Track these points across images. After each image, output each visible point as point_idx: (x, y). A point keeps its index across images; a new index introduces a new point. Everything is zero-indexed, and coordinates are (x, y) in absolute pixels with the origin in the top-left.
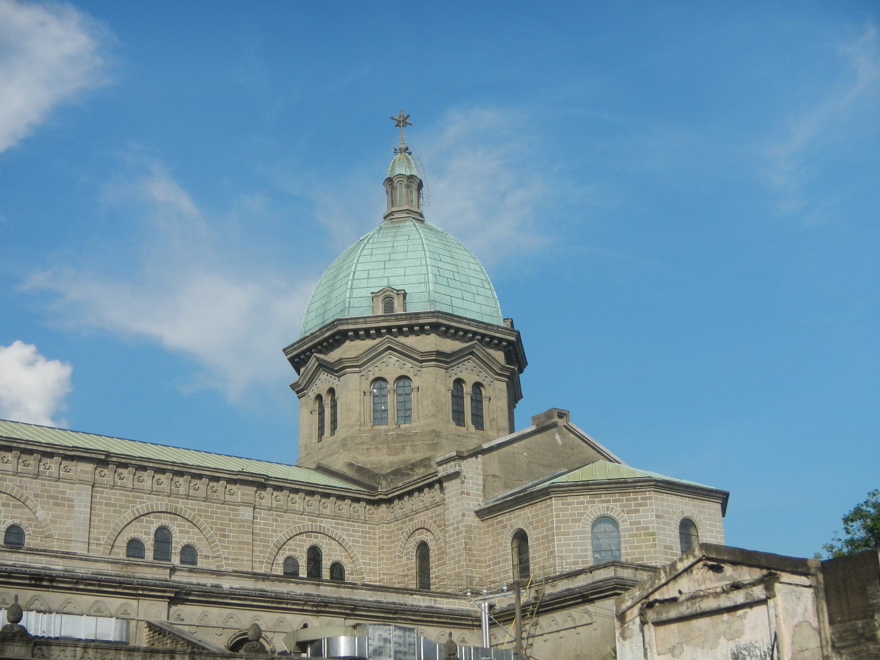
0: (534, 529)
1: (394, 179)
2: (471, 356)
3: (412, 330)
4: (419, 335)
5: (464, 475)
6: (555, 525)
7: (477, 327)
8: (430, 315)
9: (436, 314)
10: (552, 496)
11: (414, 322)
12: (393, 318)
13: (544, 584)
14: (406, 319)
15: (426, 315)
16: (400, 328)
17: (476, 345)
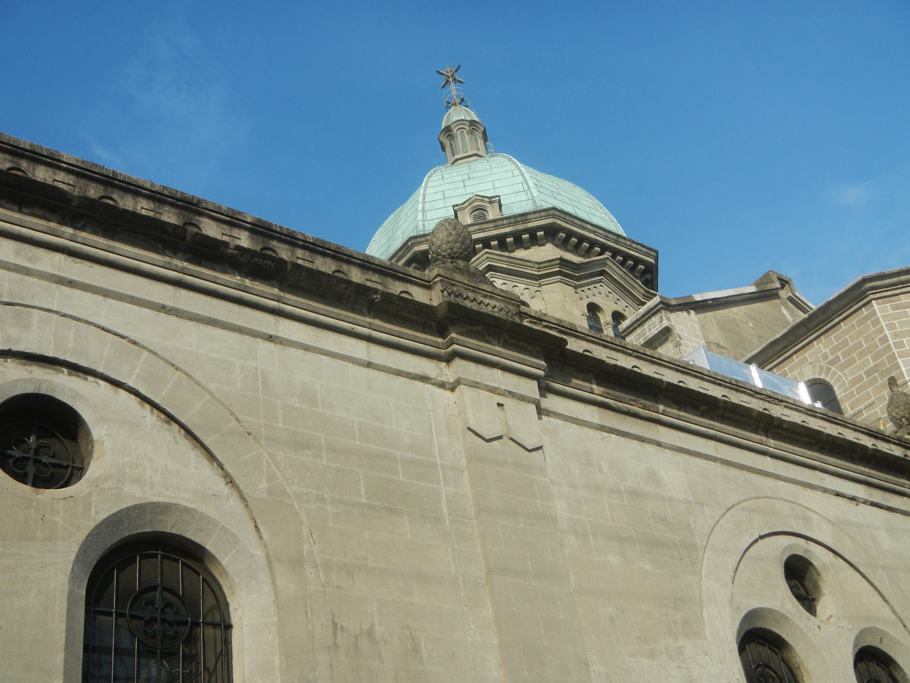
0: (842, 368)
1: (452, 127)
2: (602, 277)
3: (519, 243)
4: (529, 248)
5: (678, 334)
6: (891, 342)
8: (543, 214)
9: (552, 212)
10: (872, 297)
11: (521, 227)
12: (491, 226)
14: (509, 225)
15: (538, 215)
16: (501, 239)
17: (608, 262)
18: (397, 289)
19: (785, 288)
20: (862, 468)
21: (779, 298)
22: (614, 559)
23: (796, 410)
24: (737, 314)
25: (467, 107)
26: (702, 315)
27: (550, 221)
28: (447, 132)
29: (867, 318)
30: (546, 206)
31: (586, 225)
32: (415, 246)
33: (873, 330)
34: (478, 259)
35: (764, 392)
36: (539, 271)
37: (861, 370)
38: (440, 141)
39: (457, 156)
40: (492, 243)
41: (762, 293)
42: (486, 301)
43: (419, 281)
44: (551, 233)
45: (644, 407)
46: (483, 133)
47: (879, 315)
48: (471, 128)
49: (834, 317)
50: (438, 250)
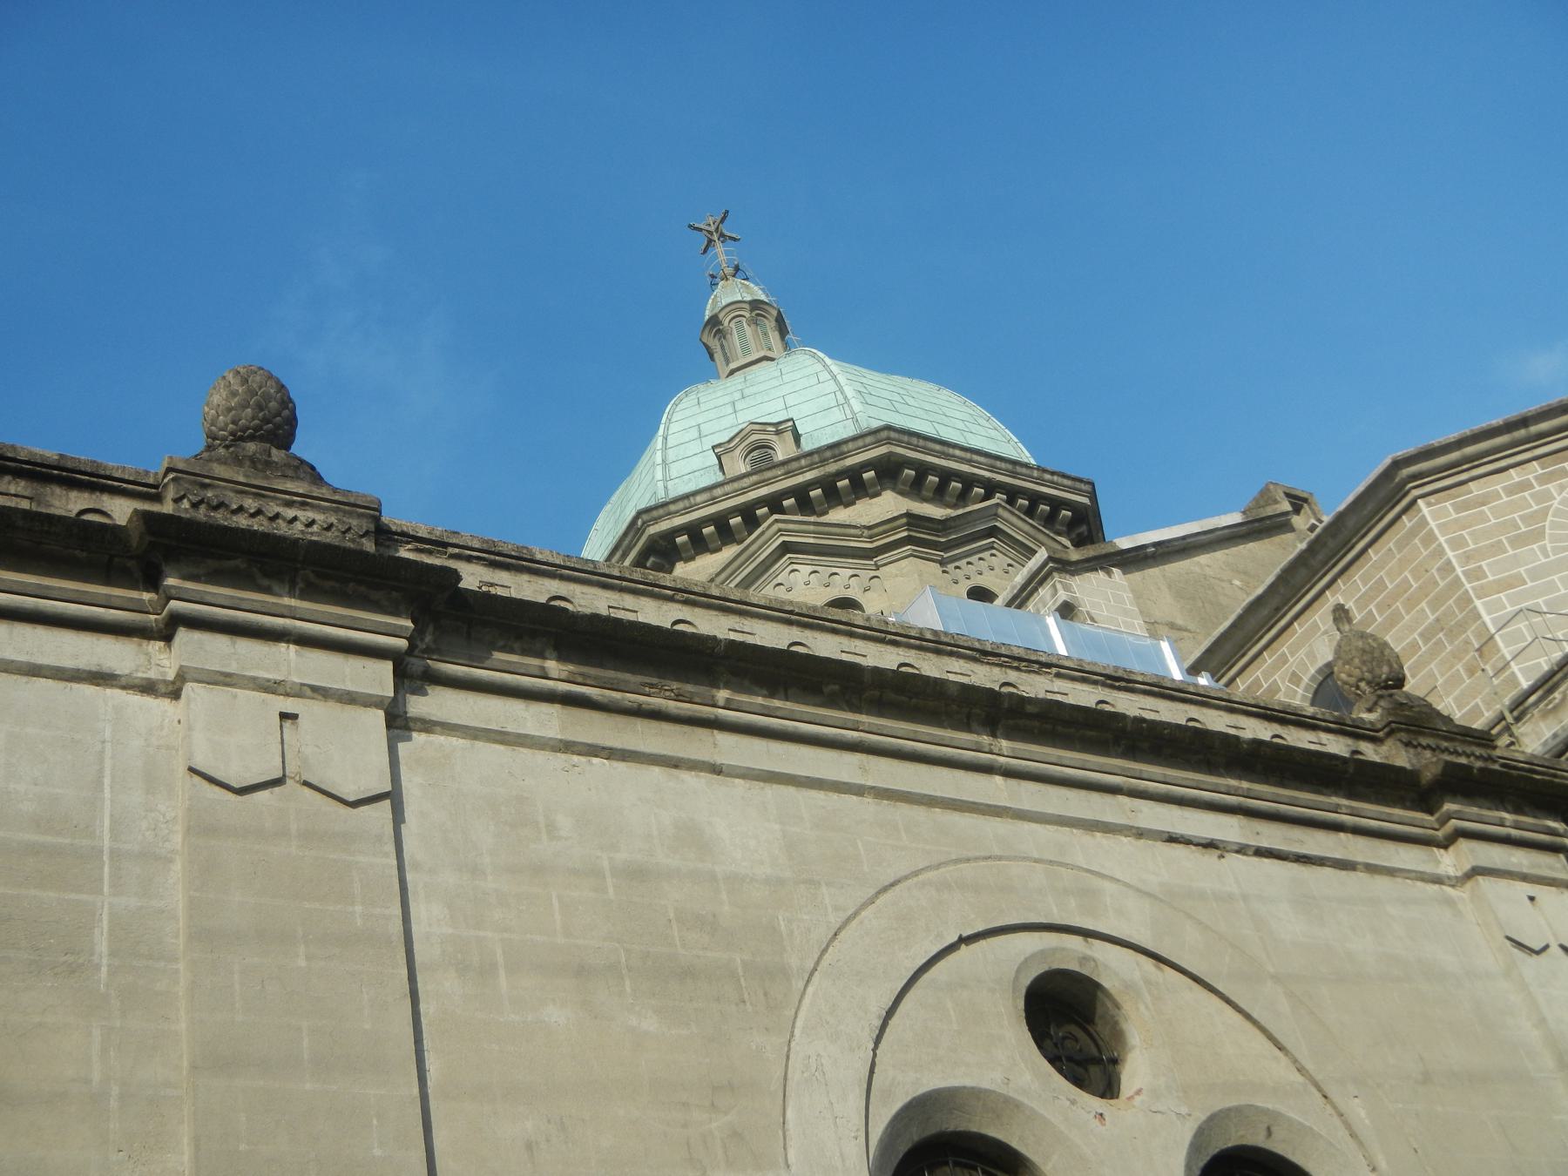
1: (721, 316)
2: (993, 539)
3: (834, 497)
4: (852, 503)
5: (1088, 613)
6: (1459, 571)
7: (992, 469)
8: (869, 440)
9: (884, 434)
10: (1416, 493)
11: (832, 468)
13: (1507, 714)
14: (811, 467)
15: (860, 443)
16: (800, 493)
17: (1000, 511)
18: (71, 506)
19: (1302, 511)
20: (1233, 782)
21: (1292, 530)
22: (556, 1015)
23: (1084, 680)
24: (1208, 566)
25: (747, 279)
26: (1137, 576)
27: (883, 450)
28: (714, 326)
29: (1413, 533)
30: (875, 424)
31: (951, 451)
32: (649, 526)
33: (1425, 553)
34: (763, 533)
35: (1003, 651)
36: (871, 542)
37: (1412, 630)
38: (704, 344)
39: (733, 366)
40: (786, 503)
41: (1257, 525)
42: (290, 513)
43: (130, 486)
44: (888, 472)
45: (679, 697)
46: (777, 320)
47: (1433, 524)
48: (753, 314)
49: (1354, 540)
50: (213, 428)
